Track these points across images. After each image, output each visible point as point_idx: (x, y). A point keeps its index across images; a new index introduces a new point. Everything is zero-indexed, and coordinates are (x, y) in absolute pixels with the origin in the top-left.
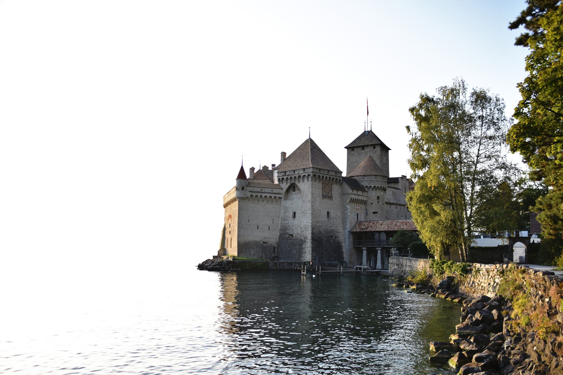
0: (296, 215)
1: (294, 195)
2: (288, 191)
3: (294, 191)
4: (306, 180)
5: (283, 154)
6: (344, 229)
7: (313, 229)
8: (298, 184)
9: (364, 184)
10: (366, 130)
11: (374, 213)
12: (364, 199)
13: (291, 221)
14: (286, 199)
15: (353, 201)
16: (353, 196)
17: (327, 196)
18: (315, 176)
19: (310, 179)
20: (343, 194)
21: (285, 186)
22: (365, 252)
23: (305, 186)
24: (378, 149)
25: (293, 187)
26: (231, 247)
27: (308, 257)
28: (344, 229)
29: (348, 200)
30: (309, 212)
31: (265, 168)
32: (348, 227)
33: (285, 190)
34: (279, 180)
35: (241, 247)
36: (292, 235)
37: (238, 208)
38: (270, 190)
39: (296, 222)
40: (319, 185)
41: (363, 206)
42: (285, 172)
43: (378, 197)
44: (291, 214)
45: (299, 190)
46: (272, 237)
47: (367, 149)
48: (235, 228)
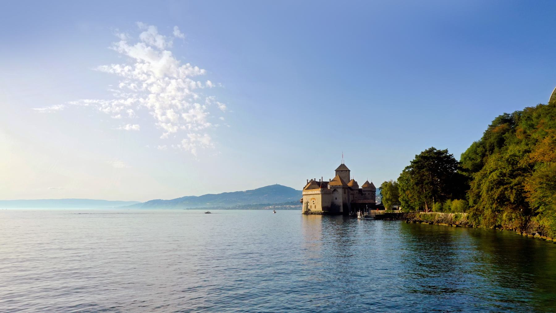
0: (337, 199)
1: (335, 192)
2: (333, 191)
3: (335, 191)
4: (340, 188)
5: (330, 179)
6: (349, 202)
7: (343, 202)
8: (337, 189)
9: (353, 188)
10: (342, 164)
11: (356, 197)
12: (353, 193)
13: (335, 201)
14: (332, 194)
15: (351, 194)
16: (351, 193)
17: (345, 193)
18: (343, 187)
19: (342, 188)
20: (348, 192)
21: (332, 190)
22: (355, 209)
23: (340, 191)
24: (348, 172)
25: (335, 190)
26: (315, 208)
27: (342, 210)
28: (349, 202)
29: (350, 194)
30: (341, 198)
31: (312, 180)
32: (350, 202)
33: (332, 191)
34: (330, 188)
35: (323, 208)
36: (335, 204)
37: (321, 197)
38: (328, 191)
39: (337, 201)
40: (343, 190)
41: (352, 195)
42: (333, 186)
43: (357, 193)
44: (335, 199)
45: (337, 191)
46: (329, 205)
47: (343, 172)
48: (319, 203)
